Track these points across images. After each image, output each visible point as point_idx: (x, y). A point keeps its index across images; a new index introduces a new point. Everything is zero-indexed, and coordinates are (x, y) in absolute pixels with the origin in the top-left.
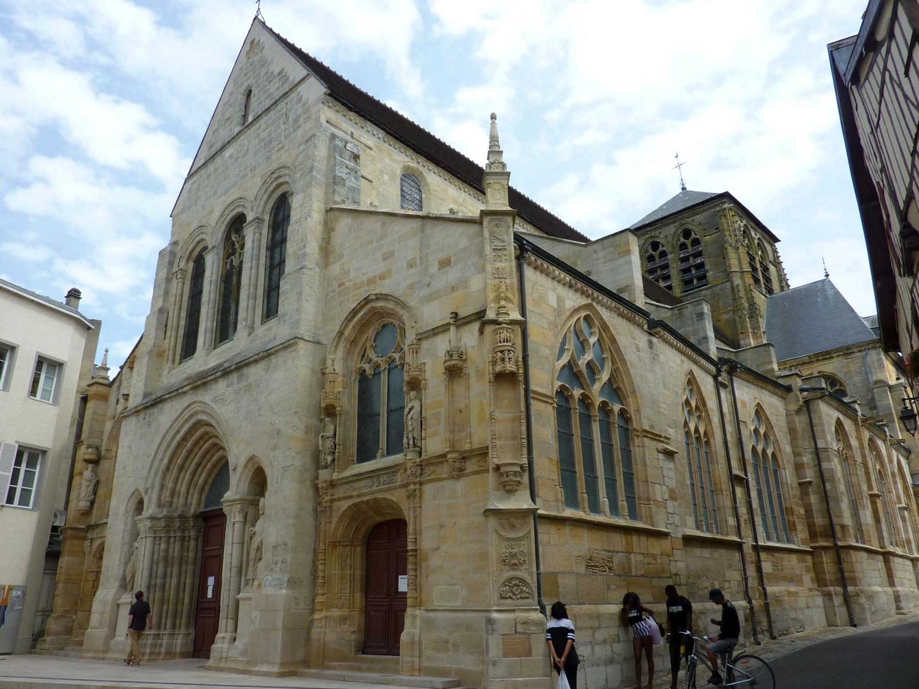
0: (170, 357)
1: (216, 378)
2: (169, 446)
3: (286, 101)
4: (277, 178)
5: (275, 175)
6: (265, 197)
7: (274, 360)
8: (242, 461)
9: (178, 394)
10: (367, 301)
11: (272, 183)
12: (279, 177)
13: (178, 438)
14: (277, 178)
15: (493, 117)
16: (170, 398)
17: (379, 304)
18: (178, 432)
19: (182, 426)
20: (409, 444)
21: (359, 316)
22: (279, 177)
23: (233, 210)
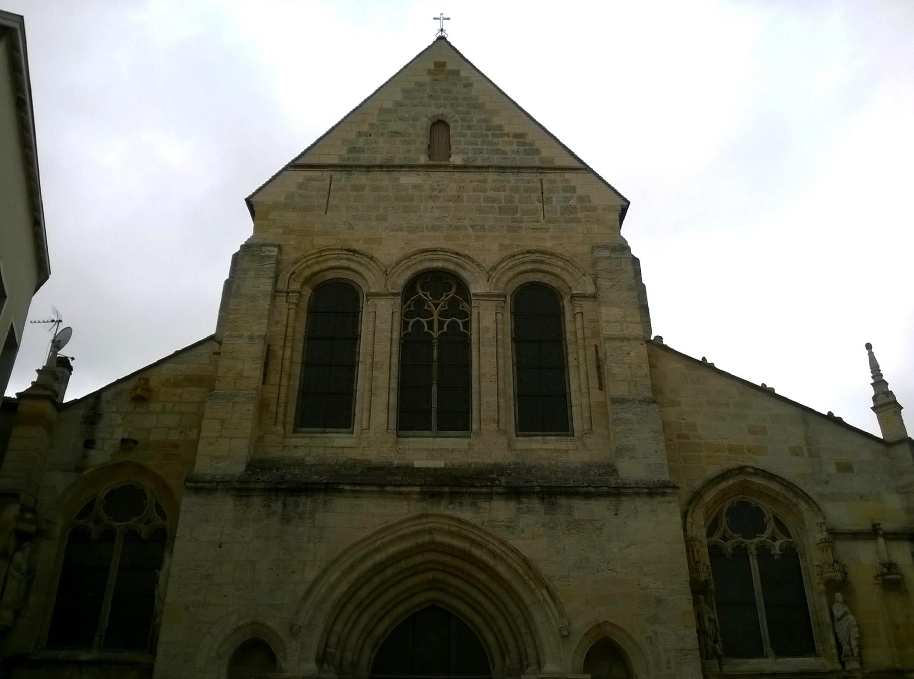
0: (281, 417)
1: (491, 493)
2: (352, 567)
3: (539, 176)
4: (534, 262)
5: (533, 257)
6: (510, 274)
7: (626, 504)
8: (580, 625)
9: (381, 492)
10: (741, 470)
11: (523, 263)
12: (542, 262)
13: (379, 557)
14: (534, 262)
15: (869, 346)
16: (353, 491)
17: (756, 480)
18: (377, 550)
19: (391, 543)
20: (851, 650)
21: (724, 485)
22: (542, 262)
23: (432, 260)
